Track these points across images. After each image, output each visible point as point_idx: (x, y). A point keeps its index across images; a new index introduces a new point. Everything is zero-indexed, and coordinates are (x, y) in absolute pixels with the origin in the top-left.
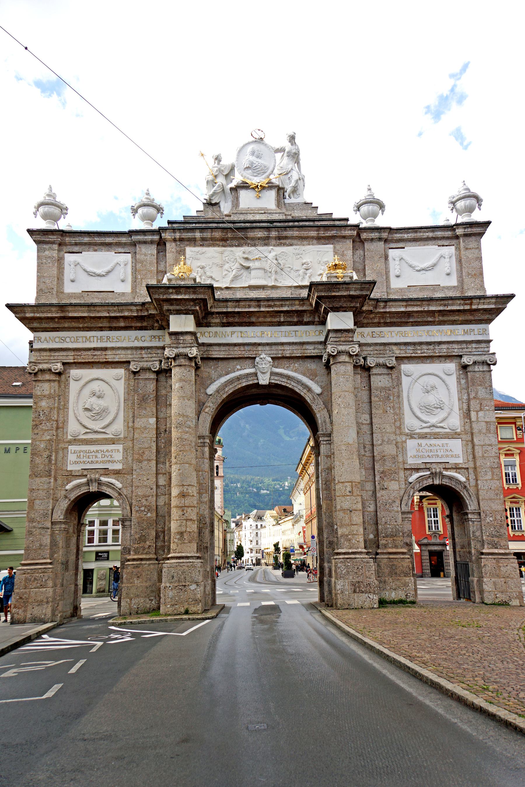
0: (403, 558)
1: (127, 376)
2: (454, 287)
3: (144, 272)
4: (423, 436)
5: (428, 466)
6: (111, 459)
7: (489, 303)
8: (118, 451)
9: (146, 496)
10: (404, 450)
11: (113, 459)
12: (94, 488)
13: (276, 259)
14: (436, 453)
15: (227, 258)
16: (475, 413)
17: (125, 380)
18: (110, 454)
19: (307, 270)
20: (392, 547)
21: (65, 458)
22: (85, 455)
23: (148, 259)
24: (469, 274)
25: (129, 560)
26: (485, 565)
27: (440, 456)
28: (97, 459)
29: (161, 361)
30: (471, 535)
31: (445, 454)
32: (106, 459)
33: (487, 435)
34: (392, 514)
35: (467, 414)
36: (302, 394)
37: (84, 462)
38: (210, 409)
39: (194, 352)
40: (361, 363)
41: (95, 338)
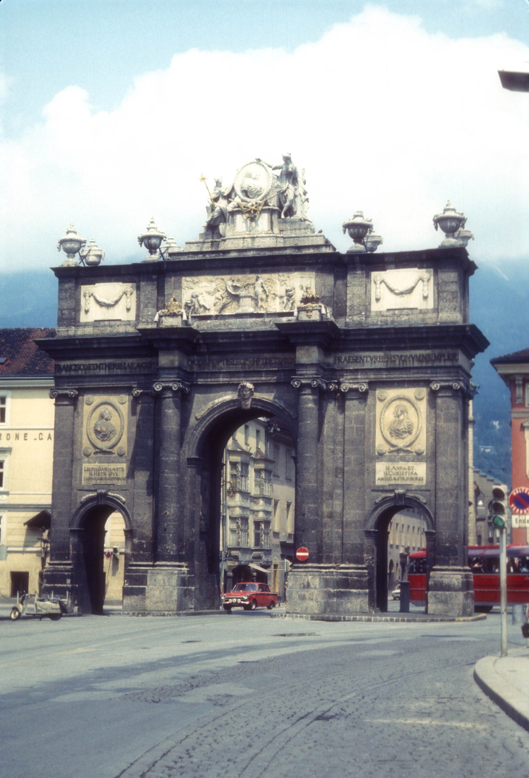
13: (262, 287)
14: (402, 476)
27: (405, 479)
31: (410, 476)
32: (112, 476)
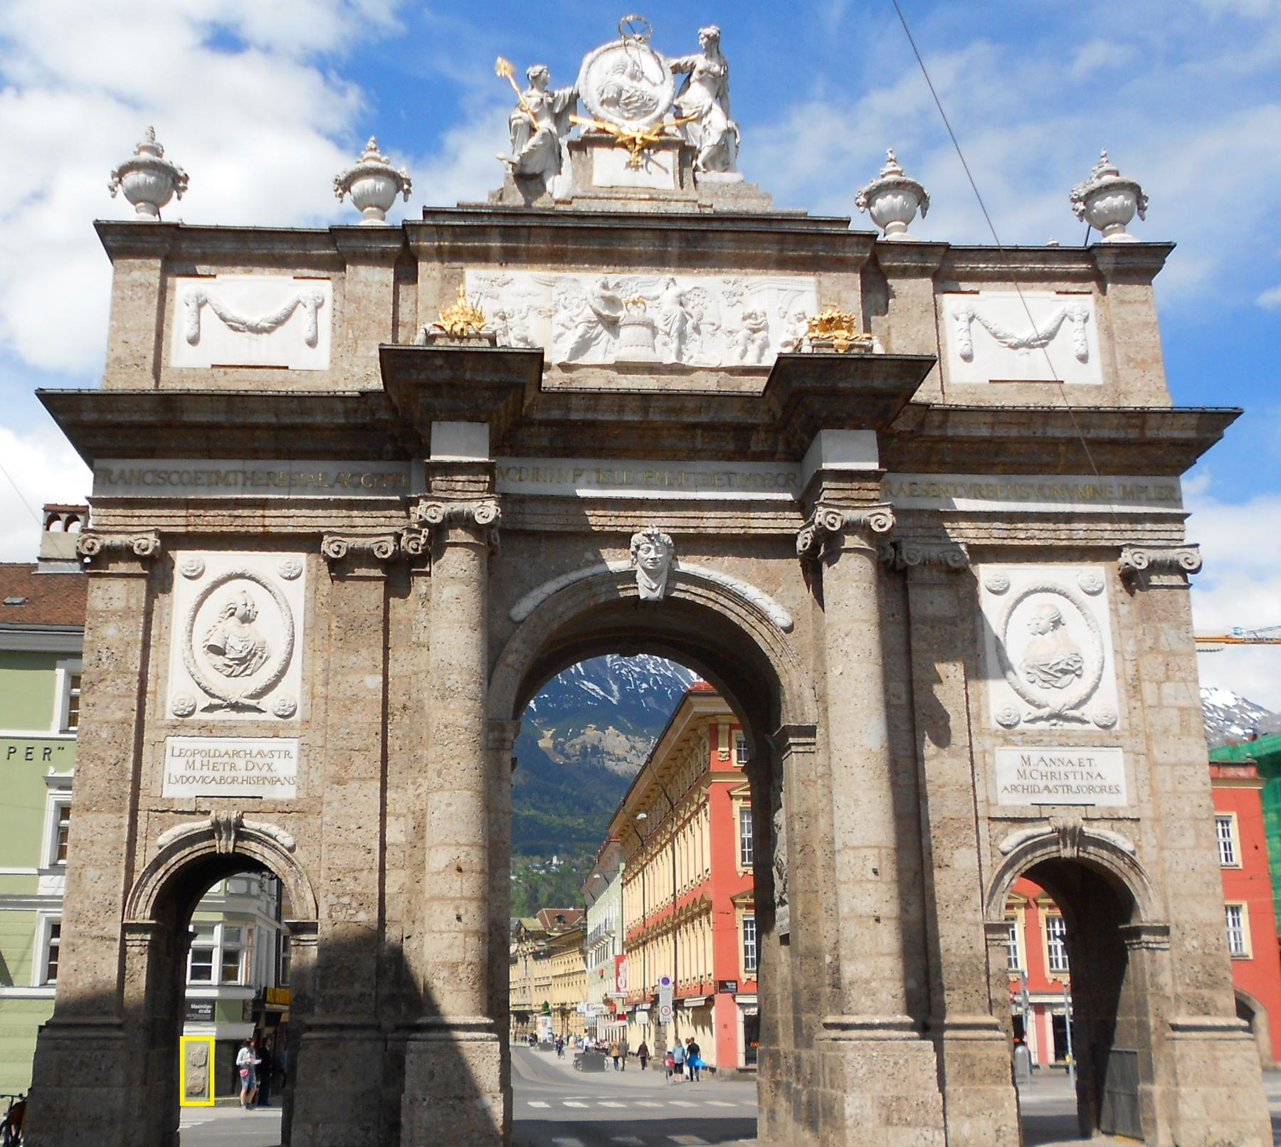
0: (990, 1039)
1: (314, 570)
2: (1098, 387)
3: (362, 324)
4: (1036, 741)
5: (1046, 812)
6: (269, 775)
7: (1184, 428)
8: (287, 753)
9: (354, 871)
10: (990, 773)
11: (274, 774)
12: (224, 845)
14: (1064, 782)
15: (562, 297)
16: (1154, 686)
17: (307, 580)
18: (268, 760)
19: (754, 331)
20: (963, 1012)
21: (159, 768)
22: (205, 762)
23: (374, 293)
24: (1129, 360)
25: (310, 1028)
26: (1182, 1056)
27: (1074, 789)
28: (233, 773)
29: (398, 537)
30: (1148, 983)
31: (1085, 783)
32: (256, 772)
33: (1184, 739)
34: (961, 930)
35: (1133, 687)
36: (745, 626)
37: (204, 779)
38: (517, 657)
39: (487, 511)
40: (888, 556)
41: (240, 477)
